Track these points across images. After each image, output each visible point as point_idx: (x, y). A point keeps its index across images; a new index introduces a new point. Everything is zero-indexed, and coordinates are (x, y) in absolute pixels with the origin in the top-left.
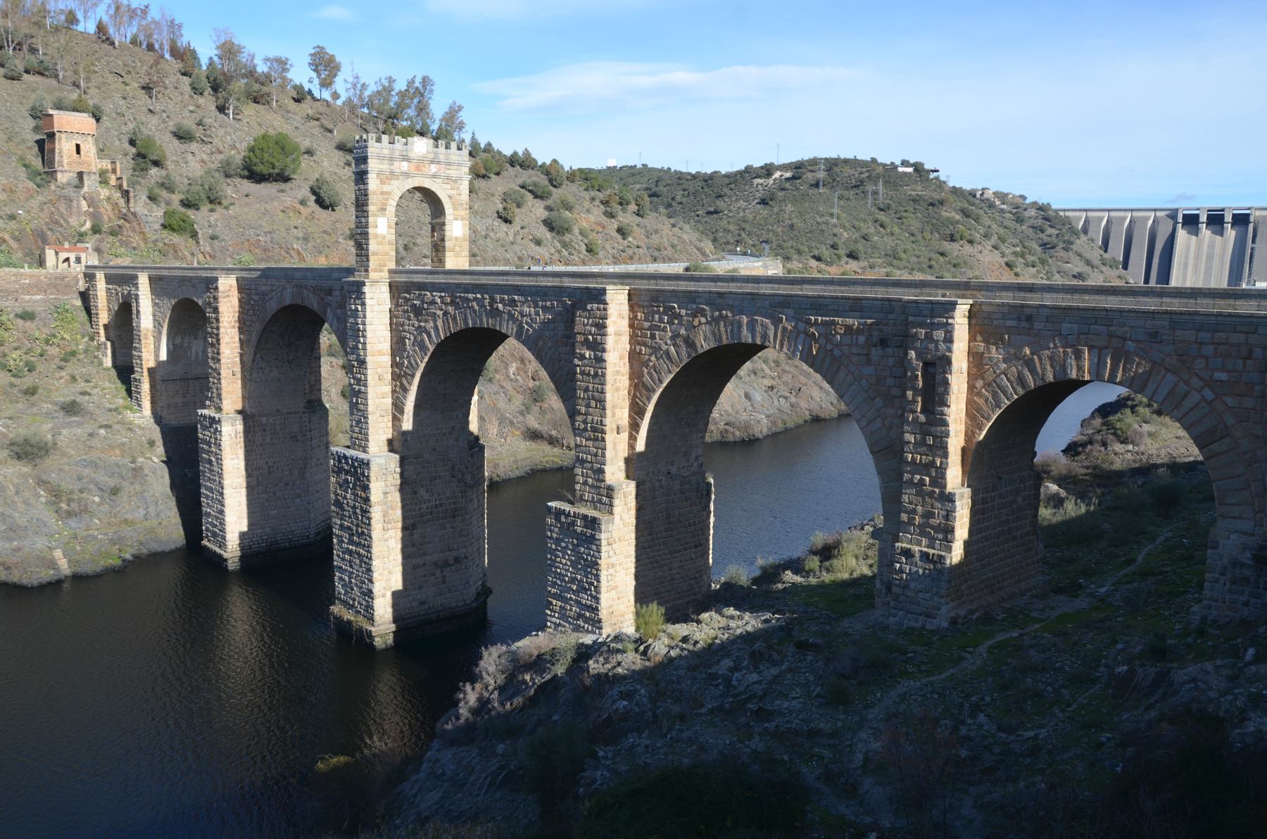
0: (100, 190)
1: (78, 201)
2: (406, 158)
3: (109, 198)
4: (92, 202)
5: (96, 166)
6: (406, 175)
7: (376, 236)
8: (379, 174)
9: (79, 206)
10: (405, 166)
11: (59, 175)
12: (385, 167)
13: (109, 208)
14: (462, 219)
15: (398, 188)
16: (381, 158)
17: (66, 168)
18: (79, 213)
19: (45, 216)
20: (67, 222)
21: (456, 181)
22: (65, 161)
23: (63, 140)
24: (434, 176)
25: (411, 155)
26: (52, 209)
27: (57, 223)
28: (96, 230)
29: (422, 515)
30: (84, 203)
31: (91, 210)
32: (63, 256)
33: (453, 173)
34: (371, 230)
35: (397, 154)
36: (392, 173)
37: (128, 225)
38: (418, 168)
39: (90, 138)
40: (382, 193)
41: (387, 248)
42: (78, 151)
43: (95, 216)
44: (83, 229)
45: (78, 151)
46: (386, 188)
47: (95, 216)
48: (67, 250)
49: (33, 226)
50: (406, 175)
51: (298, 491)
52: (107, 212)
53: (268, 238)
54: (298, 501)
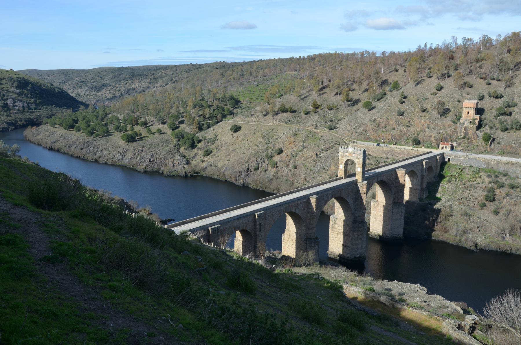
0: (469, 125)
1: (461, 129)
2: (347, 152)
3: (471, 128)
4: (466, 129)
5: (473, 117)
6: (347, 156)
7: (340, 169)
8: (341, 156)
9: (461, 130)
10: (347, 154)
11: (461, 120)
12: (343, 154)
13: (471, 131)
14: (360, 167)
15: (345, 159)
16: (342, 152)
17: (464, 118)
18: (461, 132)
19: (451, 132)
20: (457, 134)
21: (359, 158)
22: (464, 116)
23: (464, 110)
24: (353, 157)
25: (349, 152)
26: (454, 131)
27: (454, 134)
28: (464, 138)
29: (340, 232)
30: (463, 129)
31: (465, 131)
32: (443, 146)
33: (358, 156)
34: (339, 168)
35: (345, 151)
36: (344, 155)
37: (473, 137)
38: (350, 155)
39: (473, 109)
40: (342, 160)
41: (342, 172)
42: (468, 113)
43: (466, 133)
44: (461, 137)
45: (468, 113)
46: (343, 159)
47: (466, 133)
48: (444, 144)
49: (443, 136)
50: (347, 156)
51: (387, 224)
52: (470, 132)
53: (517, 145)
54: (387, 226)
